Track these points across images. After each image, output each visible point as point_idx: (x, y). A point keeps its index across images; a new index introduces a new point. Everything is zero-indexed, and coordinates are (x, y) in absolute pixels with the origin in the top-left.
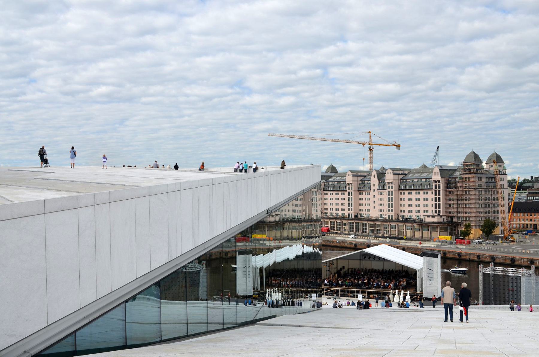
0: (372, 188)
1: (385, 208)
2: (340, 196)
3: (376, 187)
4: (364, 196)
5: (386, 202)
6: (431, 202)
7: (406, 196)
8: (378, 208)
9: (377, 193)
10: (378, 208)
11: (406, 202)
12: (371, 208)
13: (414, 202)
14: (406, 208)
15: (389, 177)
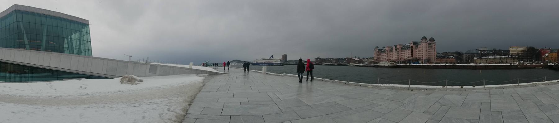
0: (393, 51)
1: (397, 57)
2: (385, 55)
3: (394, 51)
4: (391, 54)
5: (397, 55)
6: (410, 54)
7: (403, 52)
8: (395, 57)
9: (394, 52)
10: (395, 57)
11: (403, 54)
12: (393, 57)
13: (405, 54)
14: (403, 56)
15: (398, 47)
